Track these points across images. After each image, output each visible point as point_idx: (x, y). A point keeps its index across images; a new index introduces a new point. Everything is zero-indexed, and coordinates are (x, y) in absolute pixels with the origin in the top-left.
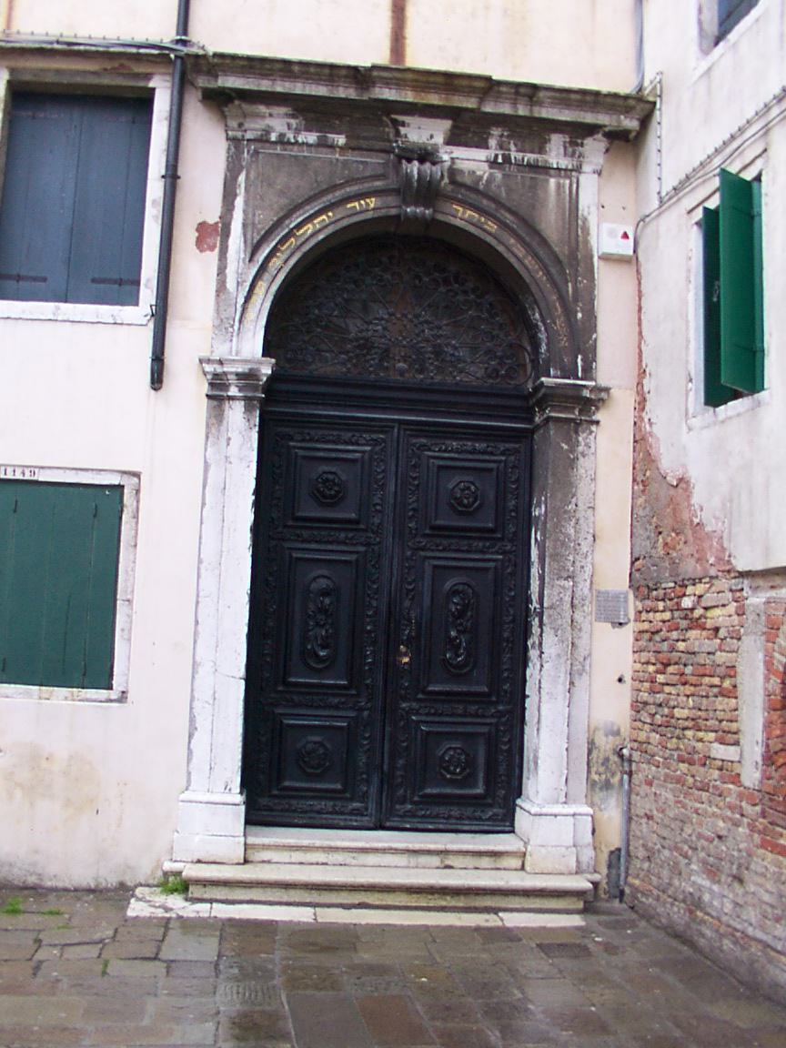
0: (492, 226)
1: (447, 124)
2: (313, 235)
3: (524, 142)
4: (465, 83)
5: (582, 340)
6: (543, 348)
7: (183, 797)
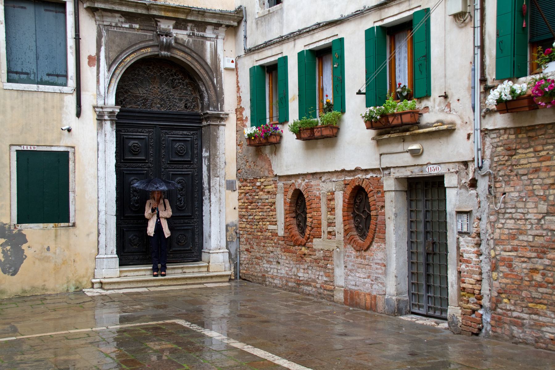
0: (189, 58)
1: (174, 22)
2: (129, 62)
3: (199, 28)
4: (181, 10)
5: (219, 97)
6: (206, 99)
7: (97, 257)
